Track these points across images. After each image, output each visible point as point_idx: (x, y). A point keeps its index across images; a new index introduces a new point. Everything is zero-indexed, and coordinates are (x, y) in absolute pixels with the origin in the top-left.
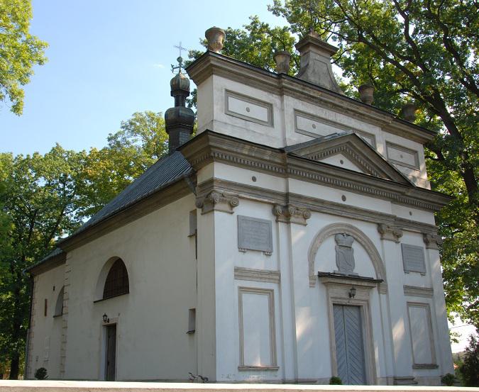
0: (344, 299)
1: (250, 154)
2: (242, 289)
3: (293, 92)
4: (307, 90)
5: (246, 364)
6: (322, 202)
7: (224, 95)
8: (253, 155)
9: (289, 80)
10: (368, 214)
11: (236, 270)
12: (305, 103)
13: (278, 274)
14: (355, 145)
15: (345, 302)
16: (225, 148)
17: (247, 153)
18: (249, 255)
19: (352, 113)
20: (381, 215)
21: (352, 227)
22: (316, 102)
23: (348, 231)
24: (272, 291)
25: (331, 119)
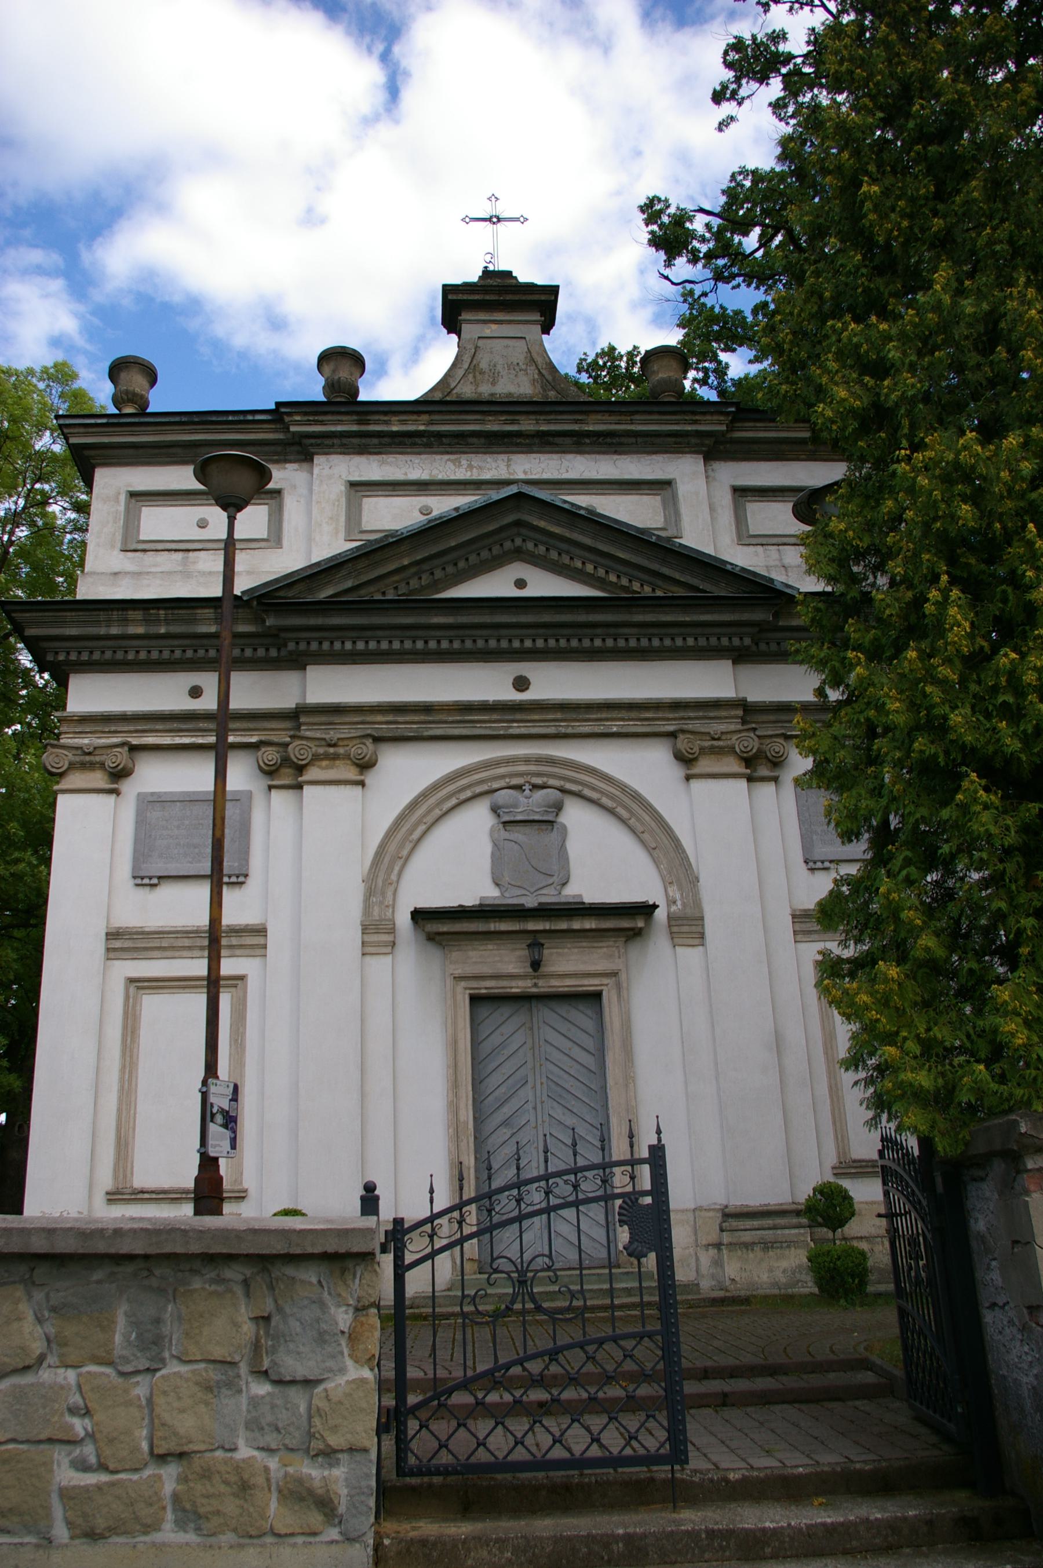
0: (512, 977)
1: (154, 630)
2: (138, 984)
3: (336, 441)
4: (377, 422)
5: (140, 1181)
6: (427, 708)
7: (122, 508)
8: (163, 630)
9: (305, 414)
10: (623, 714)
11: (113, 935)
12: (391, 458)
13: (261, 931)
14: (542, 524)
15: (517, 987)
16: (73, 631)
17: (140, 630)
18: (168, 892)
19: (568, 440)
20: (677, 705)
21: (552, 761)
22: (428, 445)
23: (539, 775)
24: (242, 978)
25: (487, 476)
